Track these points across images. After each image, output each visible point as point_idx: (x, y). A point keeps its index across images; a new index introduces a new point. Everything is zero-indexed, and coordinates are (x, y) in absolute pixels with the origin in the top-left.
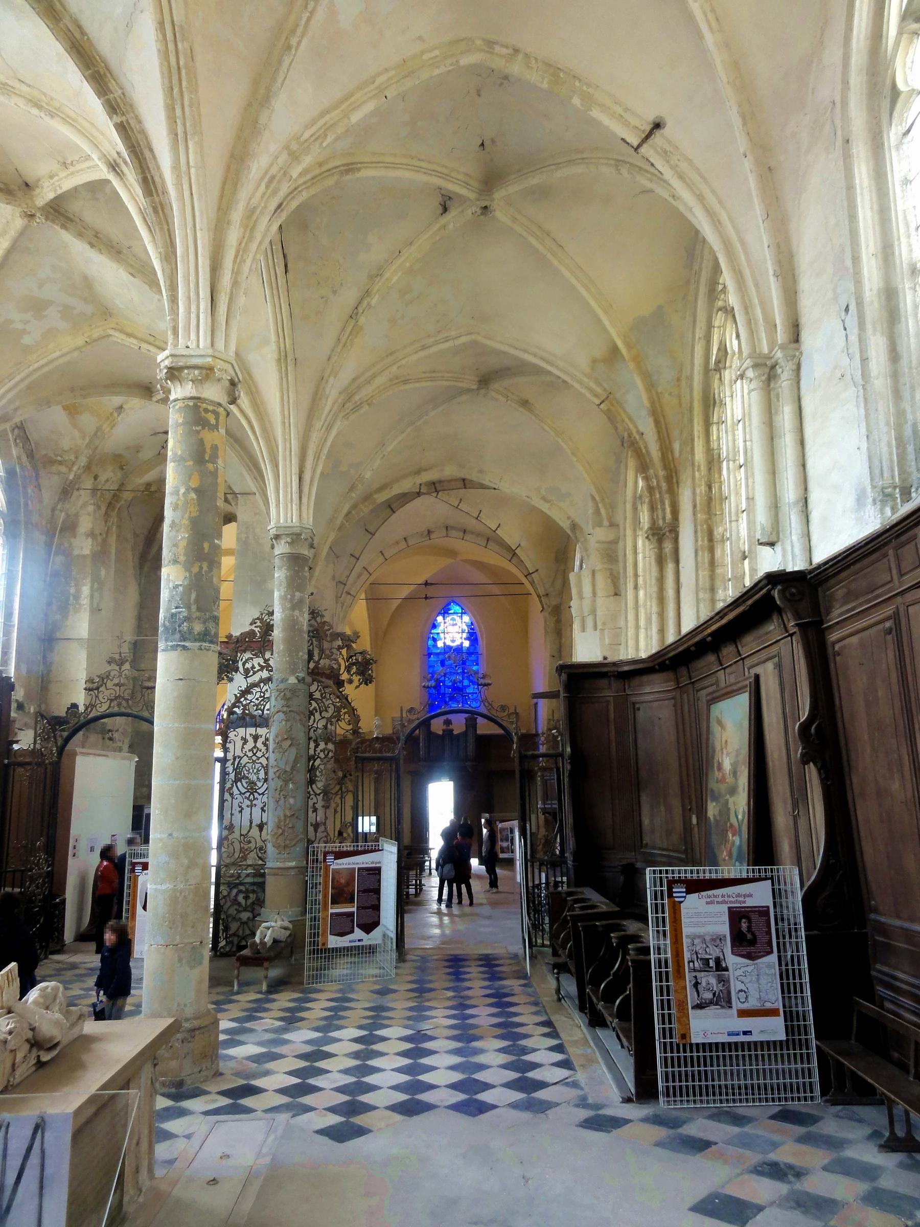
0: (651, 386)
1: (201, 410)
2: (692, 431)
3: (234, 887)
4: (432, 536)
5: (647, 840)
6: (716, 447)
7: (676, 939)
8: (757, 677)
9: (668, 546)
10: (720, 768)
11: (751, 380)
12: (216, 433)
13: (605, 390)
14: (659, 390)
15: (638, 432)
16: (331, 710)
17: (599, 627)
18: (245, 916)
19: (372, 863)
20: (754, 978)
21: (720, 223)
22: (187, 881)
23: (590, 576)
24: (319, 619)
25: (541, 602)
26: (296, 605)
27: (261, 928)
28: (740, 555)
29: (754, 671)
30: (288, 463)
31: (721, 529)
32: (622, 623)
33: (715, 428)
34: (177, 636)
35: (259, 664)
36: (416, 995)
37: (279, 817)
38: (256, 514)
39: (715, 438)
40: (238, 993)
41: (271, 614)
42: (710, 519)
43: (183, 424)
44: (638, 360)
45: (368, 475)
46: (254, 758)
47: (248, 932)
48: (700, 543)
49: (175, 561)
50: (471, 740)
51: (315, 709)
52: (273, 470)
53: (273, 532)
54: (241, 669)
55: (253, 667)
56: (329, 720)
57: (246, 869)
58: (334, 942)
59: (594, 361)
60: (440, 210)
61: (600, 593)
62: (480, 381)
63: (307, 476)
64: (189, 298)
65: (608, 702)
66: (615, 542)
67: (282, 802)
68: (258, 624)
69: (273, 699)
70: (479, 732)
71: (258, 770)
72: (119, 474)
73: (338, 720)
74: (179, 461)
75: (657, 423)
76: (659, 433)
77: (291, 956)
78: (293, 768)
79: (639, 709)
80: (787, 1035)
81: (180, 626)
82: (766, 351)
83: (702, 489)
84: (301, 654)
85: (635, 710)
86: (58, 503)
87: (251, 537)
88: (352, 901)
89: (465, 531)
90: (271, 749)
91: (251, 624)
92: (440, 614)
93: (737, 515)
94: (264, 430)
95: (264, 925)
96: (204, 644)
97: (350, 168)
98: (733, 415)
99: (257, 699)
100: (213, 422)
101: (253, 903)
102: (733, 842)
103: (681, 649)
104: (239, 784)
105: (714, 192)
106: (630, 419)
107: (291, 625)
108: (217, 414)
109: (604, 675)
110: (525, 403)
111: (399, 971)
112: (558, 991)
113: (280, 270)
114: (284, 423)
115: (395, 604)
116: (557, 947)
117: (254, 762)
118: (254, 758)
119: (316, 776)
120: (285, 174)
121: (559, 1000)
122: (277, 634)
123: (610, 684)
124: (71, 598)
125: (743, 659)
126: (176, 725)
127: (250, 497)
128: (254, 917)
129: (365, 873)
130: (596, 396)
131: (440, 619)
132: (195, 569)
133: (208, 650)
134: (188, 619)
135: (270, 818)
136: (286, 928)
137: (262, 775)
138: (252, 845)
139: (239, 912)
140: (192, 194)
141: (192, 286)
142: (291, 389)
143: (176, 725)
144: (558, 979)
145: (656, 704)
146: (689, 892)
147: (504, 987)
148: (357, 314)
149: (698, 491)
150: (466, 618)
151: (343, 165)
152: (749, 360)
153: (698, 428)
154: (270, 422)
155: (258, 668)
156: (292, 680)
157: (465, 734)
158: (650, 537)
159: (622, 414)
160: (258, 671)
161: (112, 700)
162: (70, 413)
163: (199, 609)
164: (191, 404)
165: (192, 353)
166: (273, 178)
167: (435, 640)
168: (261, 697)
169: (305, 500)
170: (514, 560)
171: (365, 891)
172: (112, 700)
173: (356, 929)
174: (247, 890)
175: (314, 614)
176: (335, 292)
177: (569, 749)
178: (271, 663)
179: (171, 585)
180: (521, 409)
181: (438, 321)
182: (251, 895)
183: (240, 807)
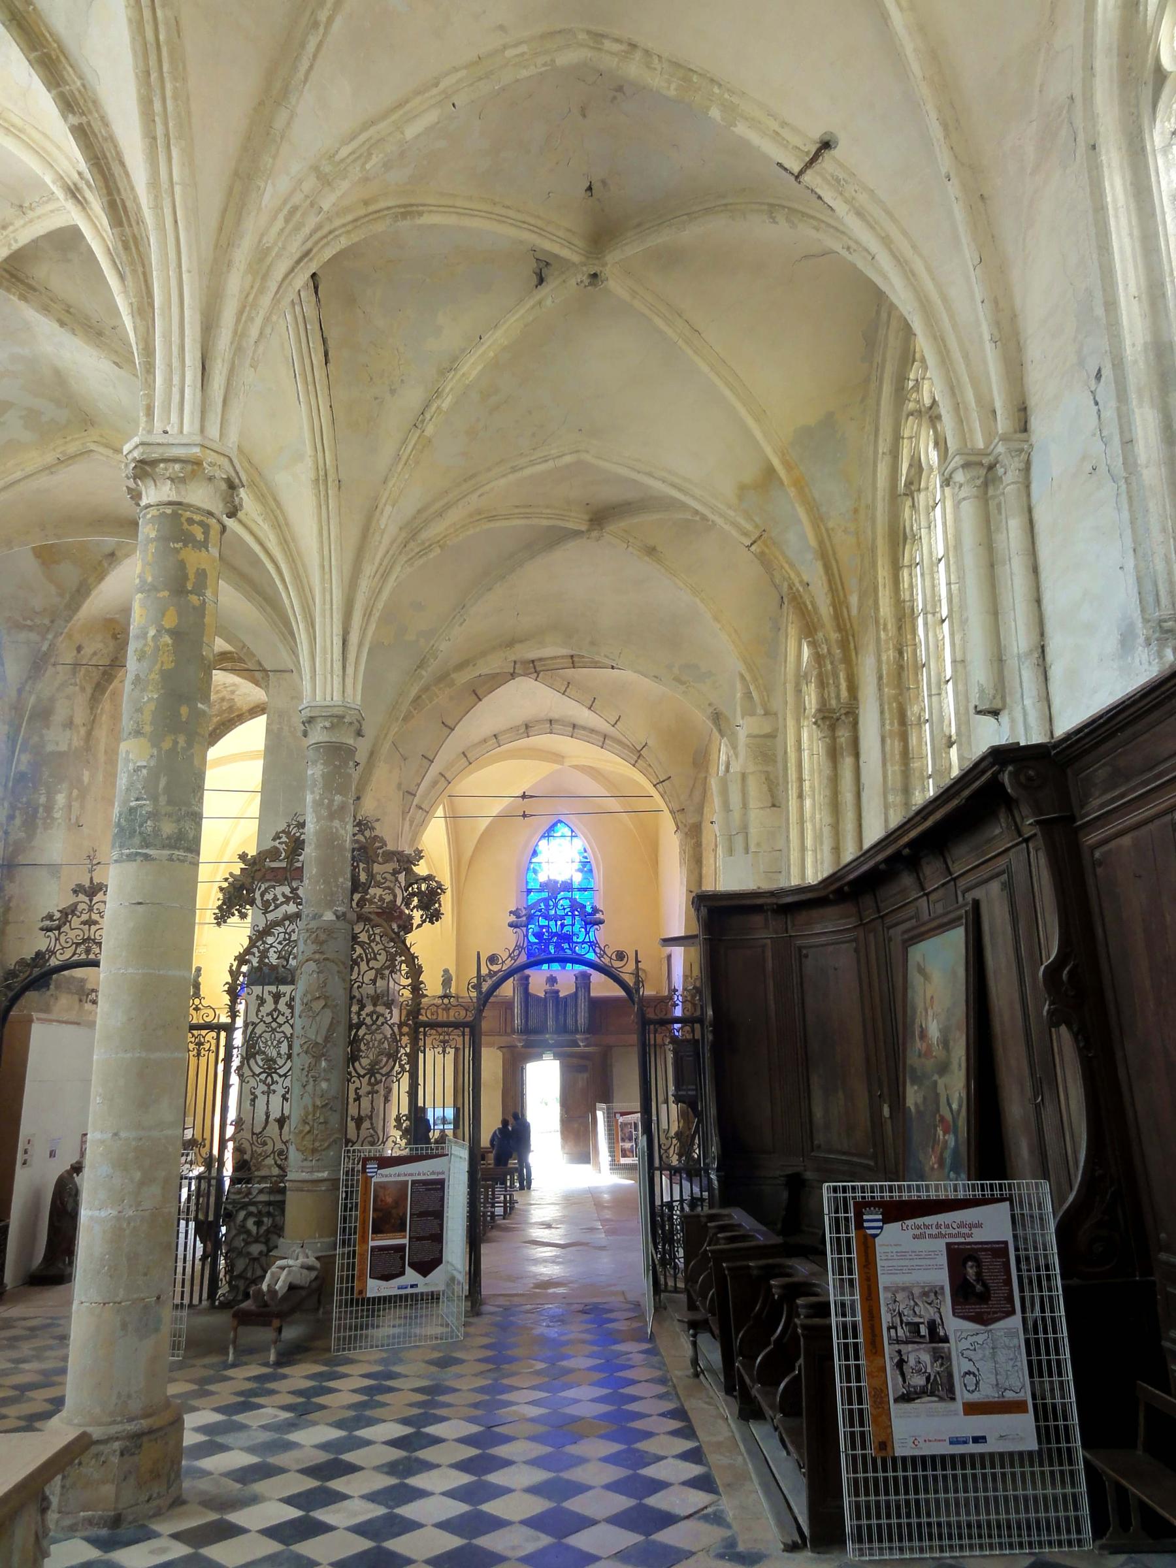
0: (818, 519)
1: (183, 520)
2: (876, 578)
3: (242, 1208)
5: (820, 1139)
6: (907, 598)
7: (870, 1294)
8: (976, 904)
9: (843, 735)
10: (923, 1035)
11: (961, 486)
12: (204, 553)
13: (757, 526)
14: (831, 525)
15: (801, 582)
16: (382, 958)
17: (753, 848)
18: (256, 1249)
19: (433, 1173)
20: (988, 1352)
21: (914, 275)
22: (139, 1204)
23: (739, 781)
24: (367, 833)
25: (674, 818)
26: (336, 813)
27: (274, 1269)
28: (944, 741)
29: (970, 896)
30: (328, 620)
31: (916, 709)
32: (780, 844)
33: (906, 572)
34: (137, 840)
35: (284, 895)
36: (492, 1366)
37: (306, 1107)
38: (292, 698)
39: (906, 586)
40: (234, 1366)
41: (302, 825)
42: (901, 694)
43: (156, 539)
44: (800, 485)
45: (444, 646)
46: (274, 1025)
47: (259, 1273)
48: (888, 727)
49: (138, 733)
50: (583, 1006)
51: (360, 956)
52: (307, 630)
53: (306, 713)
54: (258, 902)
55: (275, 899)
56: (379, 973)
57: (259, 1183)
58: (375, 1288)
59: (743, 488)
60: (535, 280)
61: (753, 804)
62: (591, 520)
63: (354, 638)
64: (170, 366)
65: (764, 946)
66: (772, 736)
67: (310, 1088)
68: (284, 839)
69: (301, 944)
71: (280, 1042)
72: (112, 643)
73: (391, 972)
74: (149, 591)
75: (827, 568)
76: (830, 581)
77: (318, 1309)
78: (327, 1039)
79: (806, 956)
80: (1040, 1442)
81: (141, 826)
82: (981, 445)
83: (889, 655)
84: (341, 880)
85: (801, 957)
86: (26, 681)
87: (286, 728)
88: (402, 1228)
89: (574, 726)
90: (297, 1013)
91: (274, 840)
92: (543, 837)
93: (940, 688)
94: (297, 577)
95: (279, 1263)
96: (177, 852)
97: (407, 211)
98: (931, 553)
99: (280, 943)
100: (200, 537)
101: (268, 1231)
102: (946, 1142)
103: (865, 868)
104: (252, 1062)
105: (905, 233)
106: (792, 565)
107: (329, 840)
108: (206, 528)
109: (758, 909)
110: (651, 551)
111: (471, 1330)
112: (695, 1362)
113: (318, 358)
114: (323, 567)
115: (484, 824)
116: (695, 1297)
117: (274, 1030)
118: (274, 1025)
119: (360, 1050)
120: (312, 205)
121: (697, 1375)
122: (309, 853)
123: (766, 920)
124: (41, 810)
125: (955, 879)
126: (130, 970)
127: (286, 675)
128: (269, 1251)
129: (422, 1188)
130: (746, 534)
132: (167, 745)
133: (183, 861)
134: (154, 815)
135: (295, 1110)
136: (310, 1268)
137: (284, 1048)
138: (269, 1148)
139: (247, 1243)
140: (176, 222)
141: (175, 349)
142: (332, 522)
143: (130, 970)
144: (694, 1344)
145: (831, 948)
146: (886, 1220)
147: (619, 1355)
148: (423, 421)
149: (884, 658)
150: (579, 843)
151: (399, 206)
152: (957, 458)
153: (883, 573)
154: (304, 565)
155: (282, 899)
156: (329, 916)
158: (819, 722)
159: (781, 558)
160: (282, 903)
161: (78, 945)
162: (43, 563)
163: (169, 802)
164: (169, 511)
165: (172, 441)
166: (295, 209)
167: (535, 872)
168: (285, 939)
169: (350, 670)
171: (421, 1214)
172: (78, 945)
173: (408, 1270)
174: (260, 1212)
175: (362, 825)
176: (393, 392)
177: (710, 1013)
178: (300, 892)
179: (131, 767)
180: (646, 558)
181: (534, 435)
182: (265, 1220)
183: (252, 1094)
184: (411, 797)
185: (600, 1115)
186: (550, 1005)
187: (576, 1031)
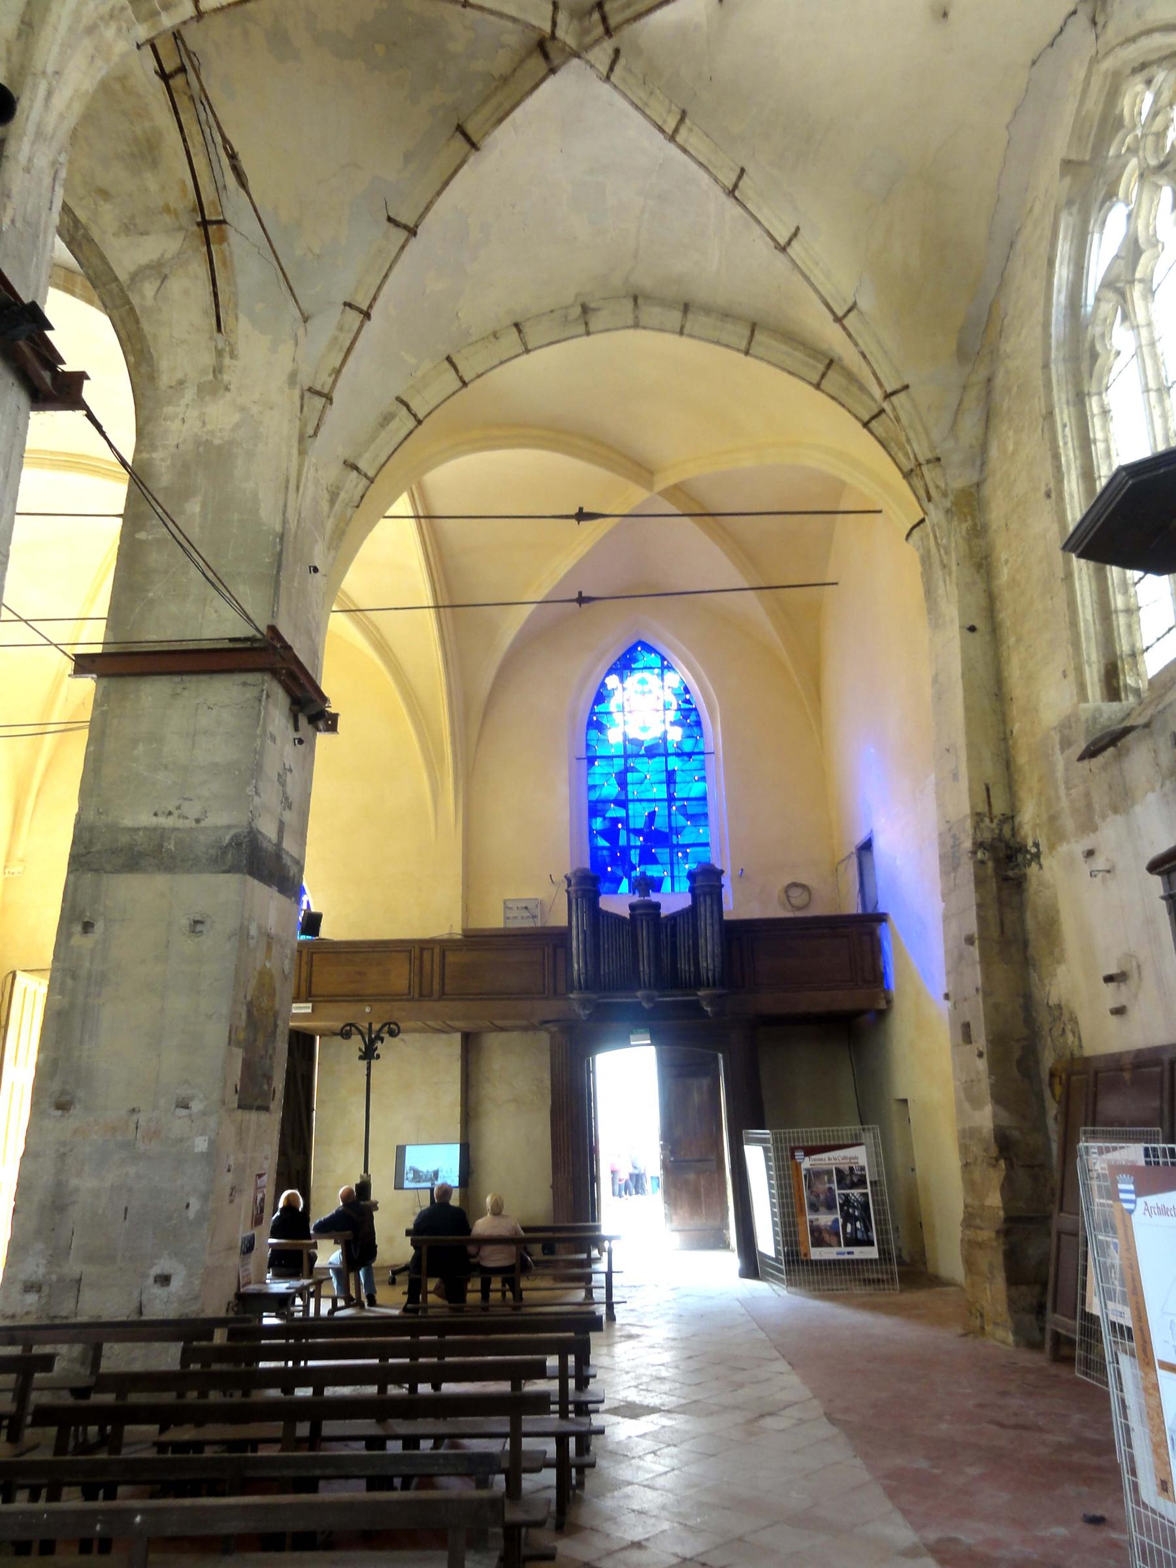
4: (595, 322)
70: (727, 916)
131: (612, 681)
157: (692, 911)
170: (834, 380)
184: (319, 402)
185: (755, 1157)
186: (644, 934)
187: (698, 983)
